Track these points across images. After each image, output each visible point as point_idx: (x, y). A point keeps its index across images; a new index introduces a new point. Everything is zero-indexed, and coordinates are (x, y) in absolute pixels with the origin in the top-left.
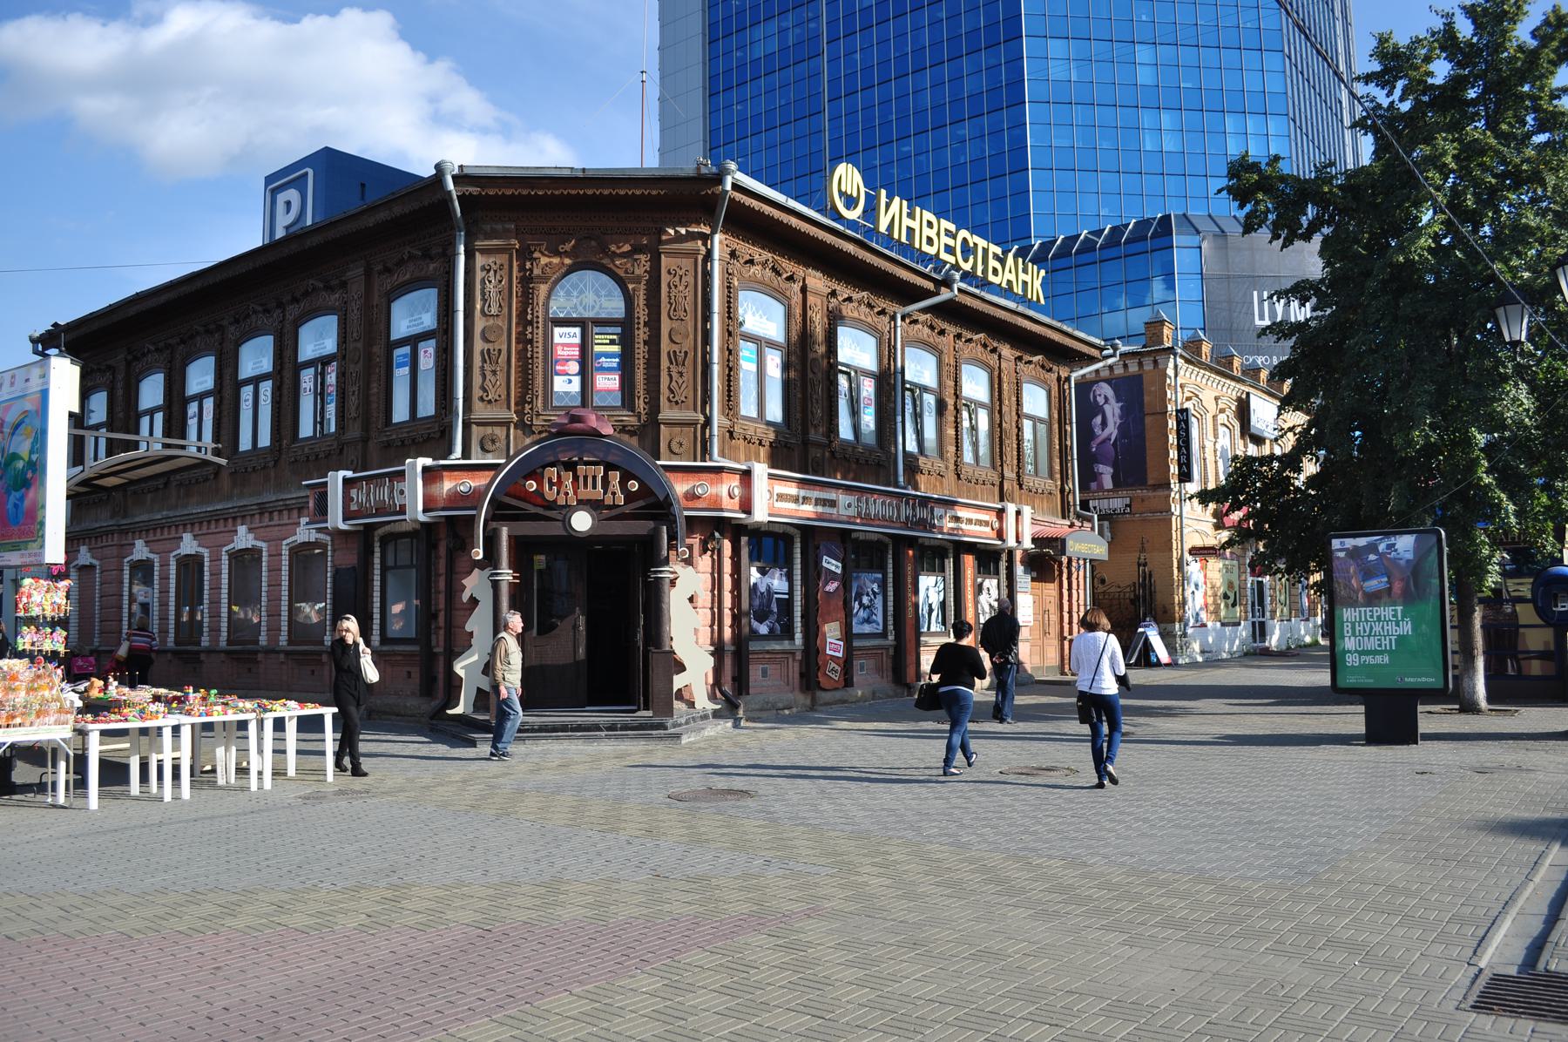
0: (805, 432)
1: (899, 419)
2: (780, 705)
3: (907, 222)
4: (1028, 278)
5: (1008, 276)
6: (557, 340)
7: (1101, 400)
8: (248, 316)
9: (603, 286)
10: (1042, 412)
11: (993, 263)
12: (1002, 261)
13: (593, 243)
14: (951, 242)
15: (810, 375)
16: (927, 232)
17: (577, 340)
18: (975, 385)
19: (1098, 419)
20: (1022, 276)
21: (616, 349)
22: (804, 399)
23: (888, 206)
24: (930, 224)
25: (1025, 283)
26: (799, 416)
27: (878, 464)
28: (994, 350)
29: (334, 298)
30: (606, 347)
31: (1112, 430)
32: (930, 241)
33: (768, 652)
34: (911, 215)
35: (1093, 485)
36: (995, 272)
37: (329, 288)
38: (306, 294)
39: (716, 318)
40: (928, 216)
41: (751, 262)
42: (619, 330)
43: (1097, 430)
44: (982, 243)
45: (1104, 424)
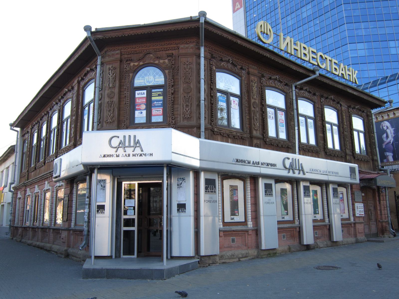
0: (251, 132)
1: (296, 128)
2: (240, 256)
3: (293, 46)
4: (350, 73)
5: (341, 72)
6: (137, 96)
7: (385, 128)
8: (53, 107)
9: (157, 74)
10: (361, 128)
11: (334, 66)
12: (339, 66)
13: (151, 55)
14: (315, 57)
15: (253, 109)
16: (303, 51)
17: (145, 96)
18: (331, 115)
19: (385, 135)
20: (347, 72)
21: (161, 98)
22: (250, 119)
23: (284, 39)
24: (305, 48)
25: (349, 75)
26: (247, 126)
27: (288, 147)
28: (338, 103)
29: (70, 95)
30: (157, 98)
31: (391, 139)
32: (305, 55)
33: (234, 231)
34: (295, 44)
35: (385, 160)
36: (336, 69)
37: (69, 91)
38: (65, 94)
39: (202, 82)
40: (303, 45)
41: (222, 60)
42: (162, 90)
43: (385, 140)
44: (329, 58)
45: (387, 137)
